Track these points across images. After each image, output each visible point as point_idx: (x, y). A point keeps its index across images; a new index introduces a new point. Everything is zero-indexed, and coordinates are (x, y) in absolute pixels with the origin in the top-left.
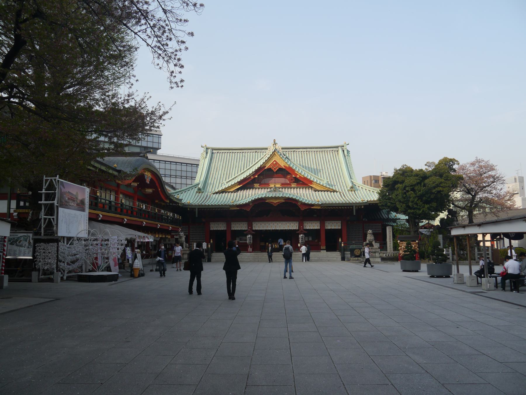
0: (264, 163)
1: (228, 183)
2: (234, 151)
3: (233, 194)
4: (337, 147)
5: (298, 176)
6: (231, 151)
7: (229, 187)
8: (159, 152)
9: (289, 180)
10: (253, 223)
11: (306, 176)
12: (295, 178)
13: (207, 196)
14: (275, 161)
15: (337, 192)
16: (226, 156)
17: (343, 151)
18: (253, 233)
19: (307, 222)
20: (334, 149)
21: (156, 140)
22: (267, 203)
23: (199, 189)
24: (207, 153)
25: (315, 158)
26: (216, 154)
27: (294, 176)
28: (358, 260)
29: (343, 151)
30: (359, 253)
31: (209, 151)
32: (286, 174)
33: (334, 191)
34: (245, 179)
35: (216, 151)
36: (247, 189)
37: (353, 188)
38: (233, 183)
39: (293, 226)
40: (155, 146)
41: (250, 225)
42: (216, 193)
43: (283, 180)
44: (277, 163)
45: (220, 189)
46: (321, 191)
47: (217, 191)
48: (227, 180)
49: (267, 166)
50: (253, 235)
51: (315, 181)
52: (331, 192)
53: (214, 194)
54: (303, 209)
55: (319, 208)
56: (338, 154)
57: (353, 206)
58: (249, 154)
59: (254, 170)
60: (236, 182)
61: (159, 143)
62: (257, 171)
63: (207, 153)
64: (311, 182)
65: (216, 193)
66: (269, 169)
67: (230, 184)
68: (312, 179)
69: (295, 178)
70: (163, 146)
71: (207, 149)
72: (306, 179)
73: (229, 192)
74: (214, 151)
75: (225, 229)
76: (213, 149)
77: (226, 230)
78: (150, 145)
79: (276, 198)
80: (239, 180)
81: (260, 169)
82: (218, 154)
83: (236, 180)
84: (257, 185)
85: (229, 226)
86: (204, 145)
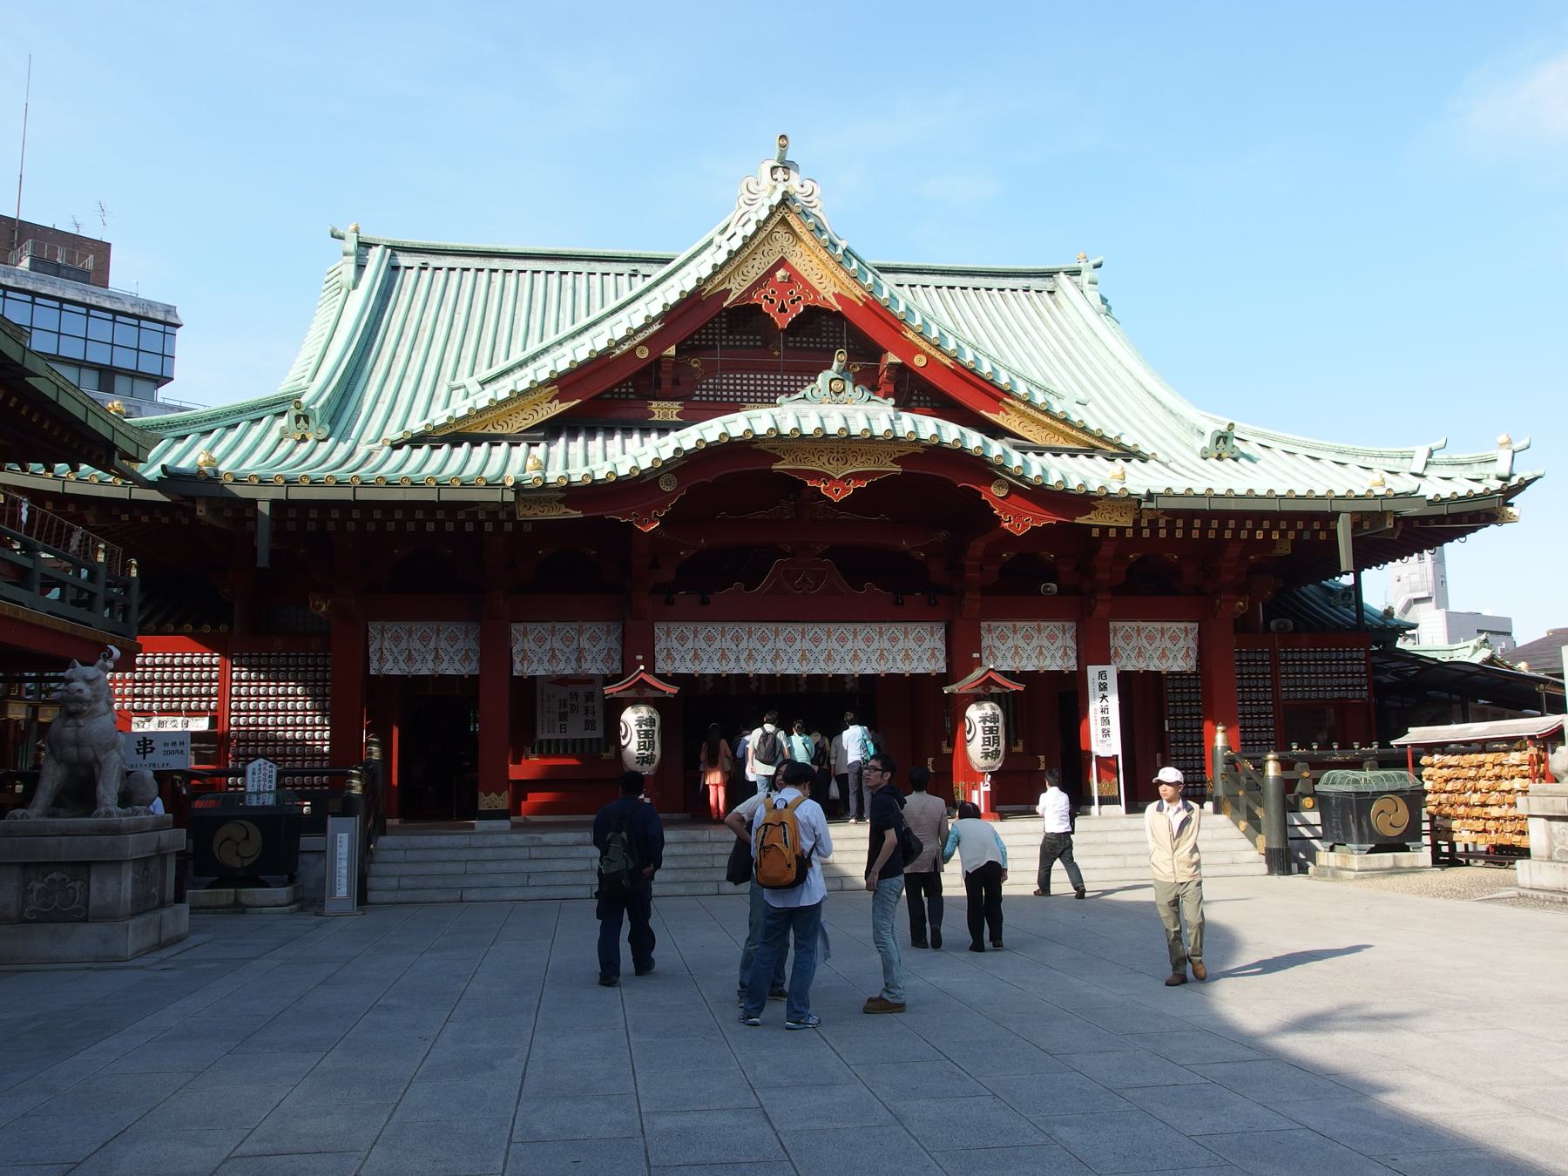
0: (717, 270)
1: (490, 389)
3: (519, 452)
4: (1049, 274)
5: (920, 361)
7: (496, 406)
8: (164, 394)
10: (660, 629)
11: (968, 358)
13: (351, 454)
14: (782, 263)
15: (1144, 459)
16: (470, 284)
18: (671, 690)
19: (1003, 626)
21: (151, 340)
22: (783, 477)
23: (303, 418)
24: (360, 267)
26: (412, 274)
27: (892, 358)
28: (1396, 870)
31: (375, 255)
32: (849, 337)
33: (1128, 454)
34: (599, 363)
35: (415, 261)
36: (609, 432)
37: (1224, 445)
38: (523, 385)
39: (910, 650)
40: (149, 365)
41: (637, 646)
42: (416, 441)
44: (794, 277)
45: (439, 417)
46: (1057, 453)
47: (416, 426)
48: (484, 373)
49: (737, 287)
50: (658, 703)
51: (1021, 388)
52: (1111, 458)
53: (396, 446)
54: (1018, 521)
55: (1126, 521)
56: (1055, 302)
57: (1335, 516)
58: (596, 280)
59: (656, 310)
60: (543, 375)
61: (166, 357)
62: (671, 315)
63: (360, 267)
64: (997, 394)
65: (416, 441)
66: (746, 316)
67: (502, 390)
68: (1003, 379)
69: (902, 370)
70: (180, 369)
71: (365, 246)
72: (968, 375)
73: (494, 440)
74: (403, 260)
75: (469, 668)
76: (396, 249)
77: (473, 680)
78: (124, 360)
79: (846, 445)
80: (563, 366)
81: (691, 301)
82: (426, 275)
83: (542, 371)
84: (664, 410)
85: (496, 650)
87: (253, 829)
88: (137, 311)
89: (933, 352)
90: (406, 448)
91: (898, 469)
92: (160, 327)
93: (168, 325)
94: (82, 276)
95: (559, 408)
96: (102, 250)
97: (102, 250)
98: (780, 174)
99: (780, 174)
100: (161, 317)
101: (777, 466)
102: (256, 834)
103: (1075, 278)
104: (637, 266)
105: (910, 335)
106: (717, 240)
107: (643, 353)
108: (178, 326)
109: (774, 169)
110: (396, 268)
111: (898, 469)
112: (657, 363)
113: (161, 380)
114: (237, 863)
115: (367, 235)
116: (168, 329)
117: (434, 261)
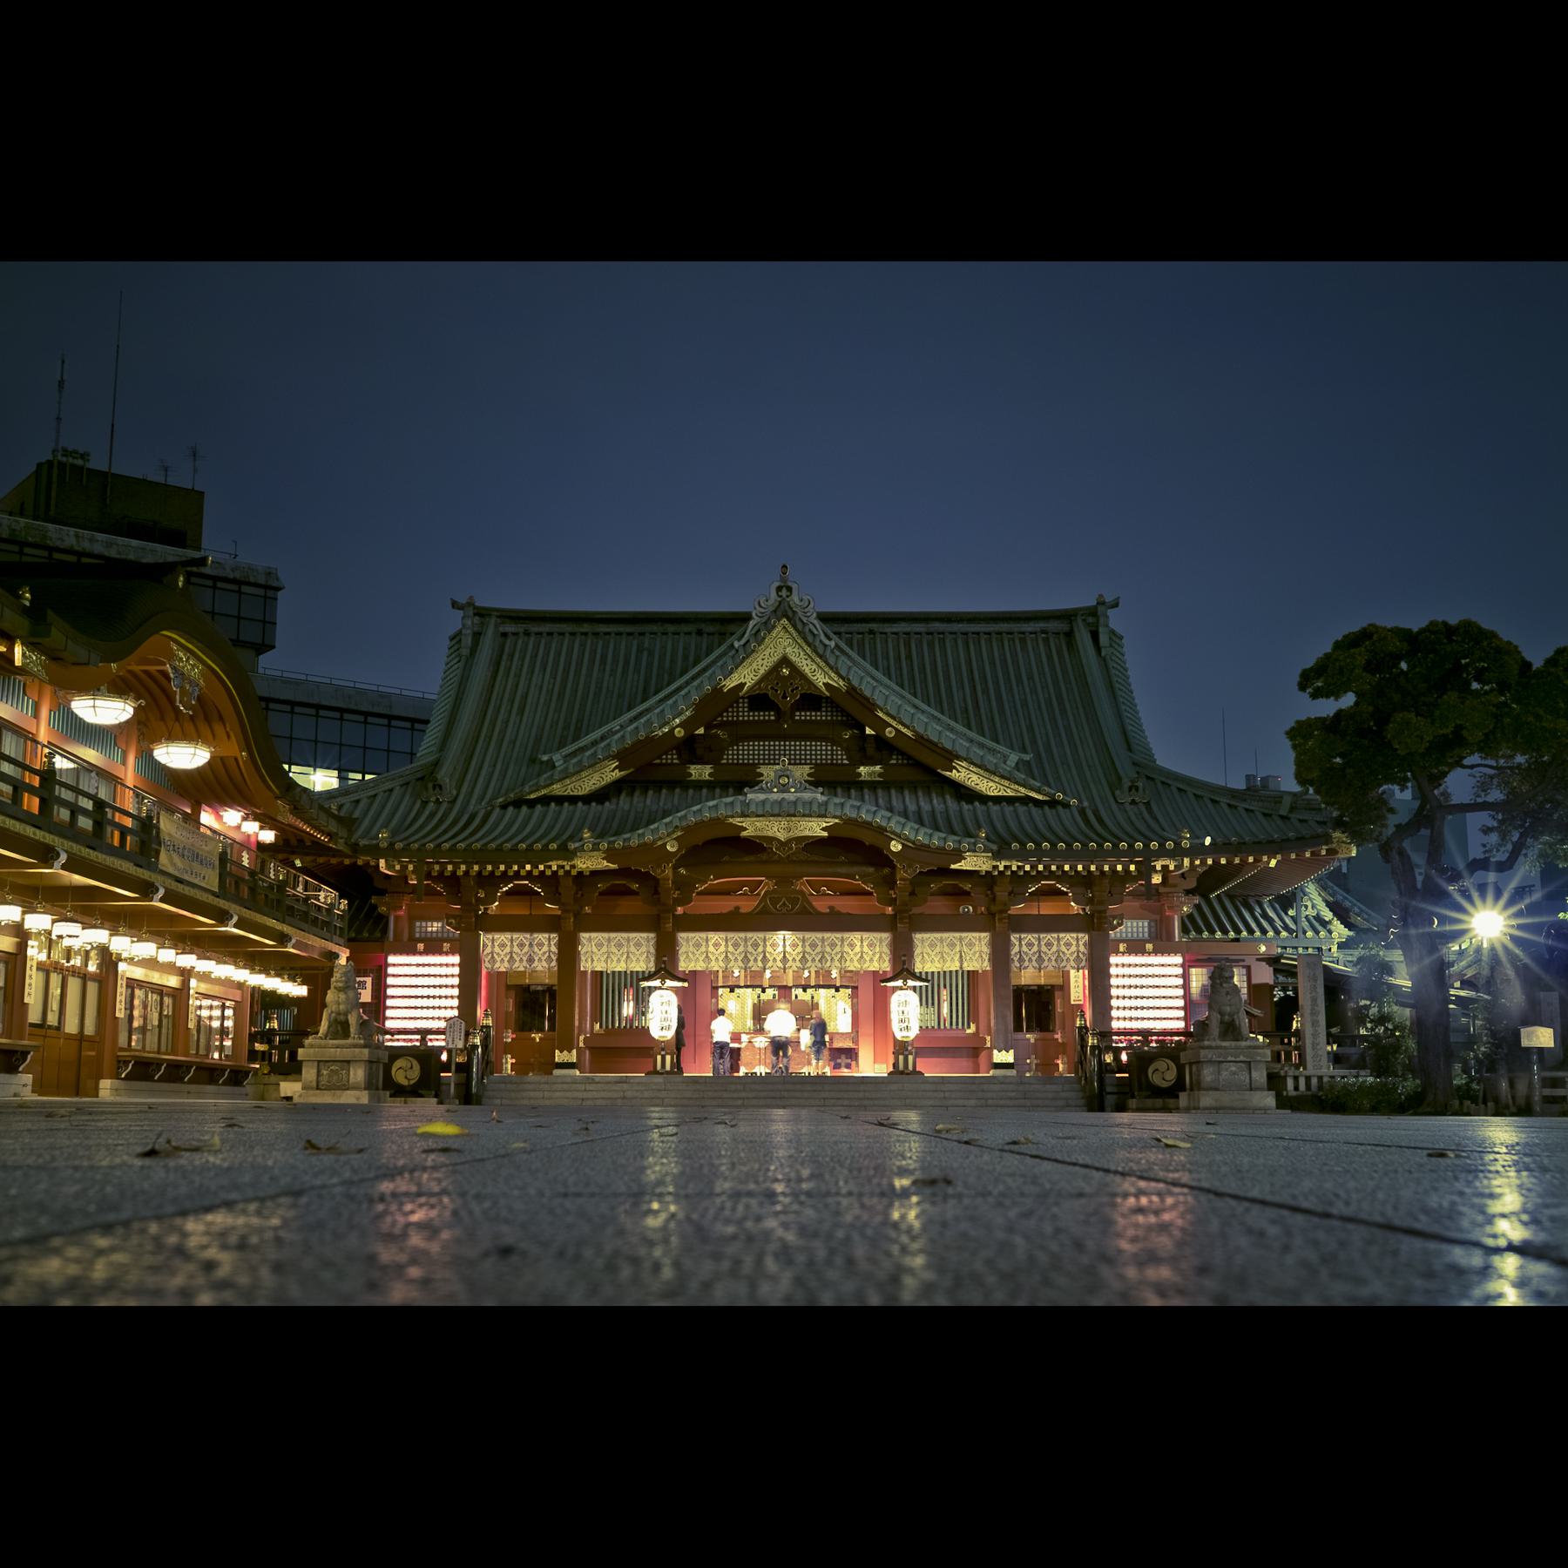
2: (603, 628)
4: (1068, 616)
6: (586, 628)
9: (847, 751)
12: (879, 740)
14: (785, 661)
17: (1095, 636)
20: (1053, 626)
25: (969, 662)
27: (868, 731)
29: (1095, 636)
30: (1171, 1075)
43: (822, 751)
44: (796, 671)
61: (268, 624)
71: (482, 613)
74: (510, 628)
85: (568, 955)
86: (463, 600)
87: (415, 1063)
88: (237, 575)
89: (900, 727)
90: (511, 809)
91: (825, 834)
92: (261, 592)
93: (269, 590)
94: (176, 538)
95: (617, 774)
96: (195, 498)
97: (195, 498)
98: (784, 593)
99: (784, 593)
100: (262, 581)
101: (744, 834)
102: (417, 1067)
103: (1090, 620)
104: (703, 626)
105: (880, 714)
106: (736, 644)
107: (679, 733)
108: (278, 589)
109: (779, 589)
110: (504, 635)
111: (825, 834)
112: (690, 740)
113: (264, 647)
114: (405, 1082)
115: (482, 602)
116: (270, 593)
117: (535, 628)
